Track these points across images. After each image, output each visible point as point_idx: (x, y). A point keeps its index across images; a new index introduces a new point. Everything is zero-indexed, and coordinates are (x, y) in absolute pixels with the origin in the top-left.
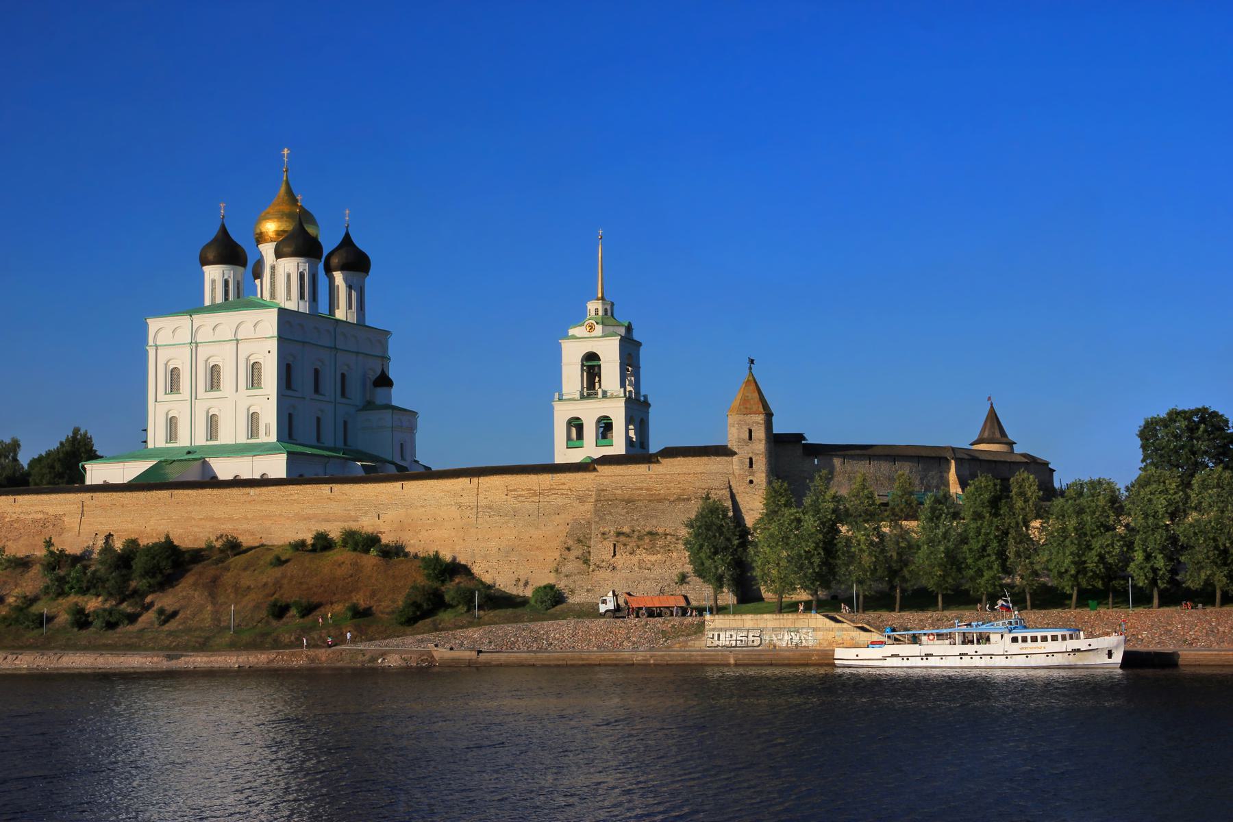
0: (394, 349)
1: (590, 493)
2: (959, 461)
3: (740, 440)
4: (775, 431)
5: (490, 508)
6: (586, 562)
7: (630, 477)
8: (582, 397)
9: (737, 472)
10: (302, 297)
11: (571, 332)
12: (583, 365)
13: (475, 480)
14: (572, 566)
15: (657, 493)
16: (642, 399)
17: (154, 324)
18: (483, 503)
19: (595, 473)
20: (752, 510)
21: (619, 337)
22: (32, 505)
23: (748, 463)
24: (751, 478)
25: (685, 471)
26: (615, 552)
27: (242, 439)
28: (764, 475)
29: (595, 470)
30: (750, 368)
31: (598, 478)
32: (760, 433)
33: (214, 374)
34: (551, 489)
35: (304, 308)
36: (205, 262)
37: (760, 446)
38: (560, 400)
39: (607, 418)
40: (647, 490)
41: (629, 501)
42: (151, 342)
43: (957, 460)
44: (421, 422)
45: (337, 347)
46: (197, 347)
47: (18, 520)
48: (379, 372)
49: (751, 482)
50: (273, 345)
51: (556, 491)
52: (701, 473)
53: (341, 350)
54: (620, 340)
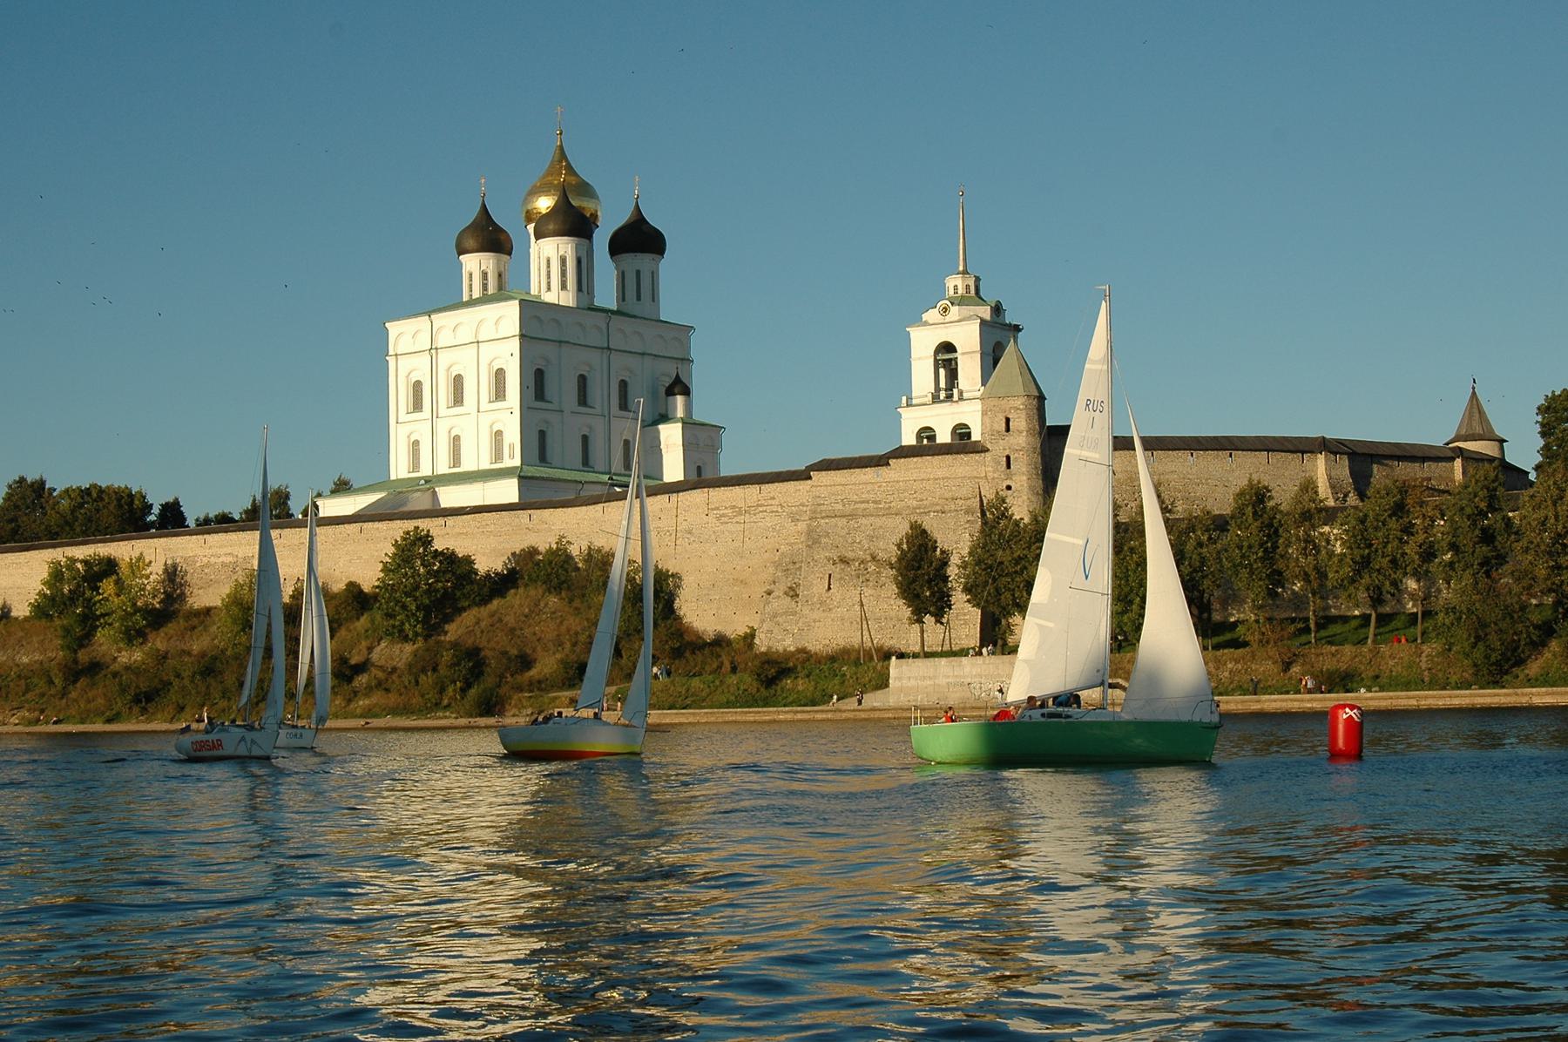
1: (805, 509)
7: (853, 487)
10: (564, 287)
11: (925, 317)
12: (936, 361)
14: (781, 603)
15: (887, 506)
17: (394, 328)
18: (684, 526)
19: (809, 482)
24: (1008, 483)
26: (829, 584)
27: (485, 464)
29: (810, 478)
31: (814, 489)
32: (1020, 422)
33: (458, 381)
34: (758, 505)
35: (568, 299)
36: (462, 251)
40: (874, 502)
41: (852, 516)
44: (726, 438)
45: (611, 347)
46: (437, 354)
47: (208, 565)
50: (515, 345)
51: (765, 508)
52: (943, 479)
53: (616, 350)
54: (981, 324)
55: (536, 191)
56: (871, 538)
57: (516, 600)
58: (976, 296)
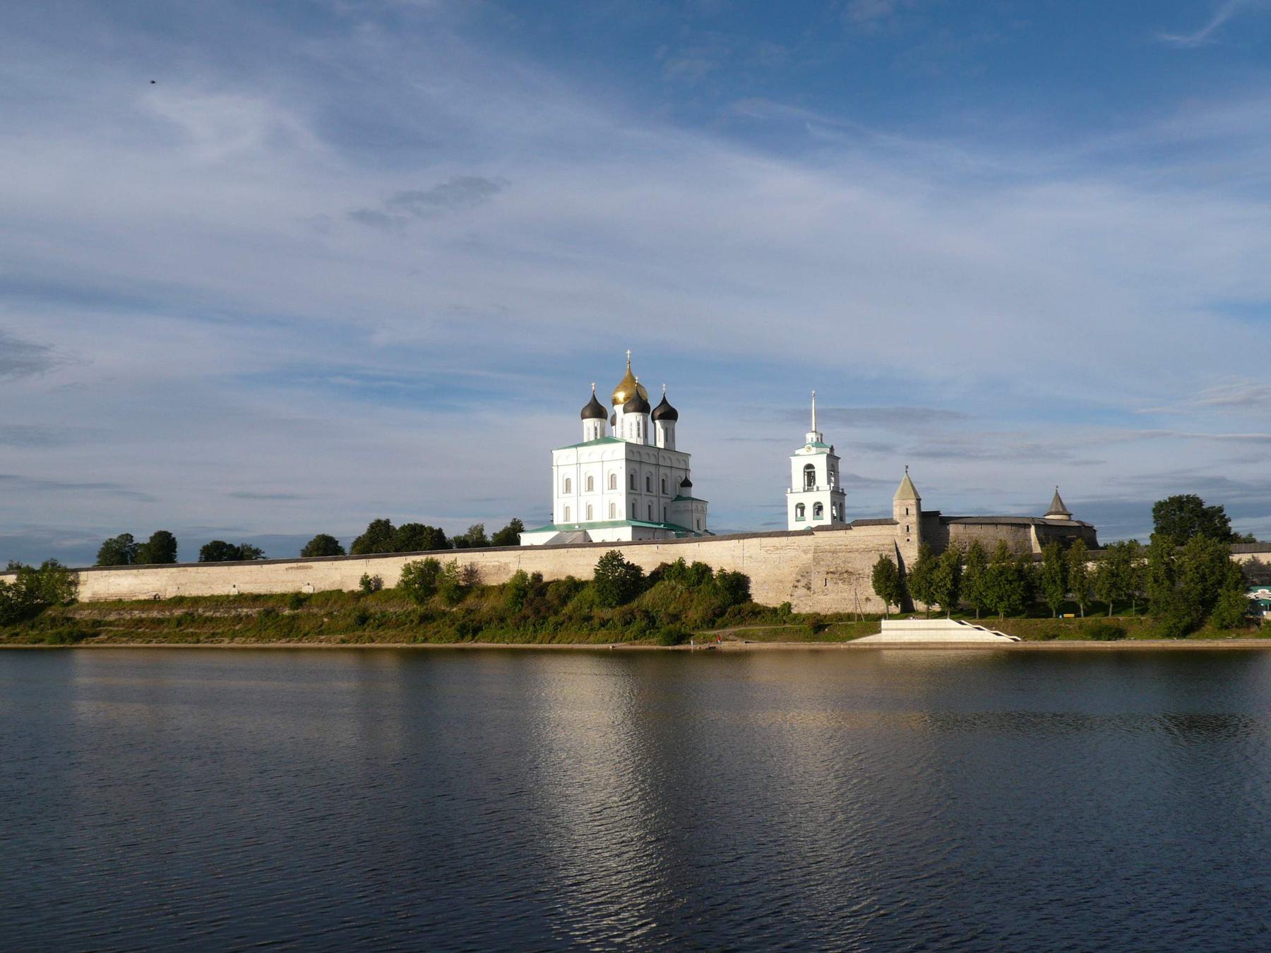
0: (692, 463)
2: (1037, 526)
3: (901, 515)
4: (922, 510)
5: (751, 557)
6: (809, 589)
8: (804, 491)
9: (899, 535)
10: (639, 435)
12: (804, 472)
13: (741, 541)
14: (802, 591)
16: (841, 491)
18: (747, 554)
20: (909, 557)
21: (826, 455)
22: (492, 557)
23: (906, 529)
24: (908, 538)
25: (869, 534)
27: (606, 519)
28: (916, 536)
29: (813, 534)
30: (907, 472)
32: (913, 511)
33: (590, 480)
35: (640, 442)
36: (583, 417)
37: (913, 519)
38: (791, 493)
39: (819, 503)
41: (834, 552)
42: (554, 464)
43: (1035, 525)
47: (485, 566)
48: (684, 478)
49: (908, 540)
50: (623, 463)
54: (827, 456)
55: (617, 390)
56: (844, 562)
57: (660, 586)
58: (819, 443)
